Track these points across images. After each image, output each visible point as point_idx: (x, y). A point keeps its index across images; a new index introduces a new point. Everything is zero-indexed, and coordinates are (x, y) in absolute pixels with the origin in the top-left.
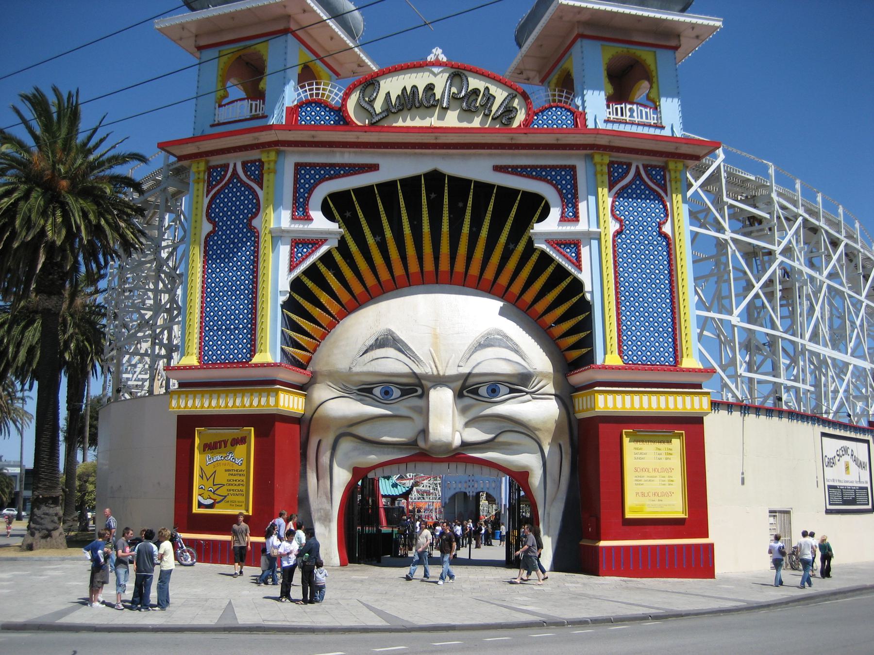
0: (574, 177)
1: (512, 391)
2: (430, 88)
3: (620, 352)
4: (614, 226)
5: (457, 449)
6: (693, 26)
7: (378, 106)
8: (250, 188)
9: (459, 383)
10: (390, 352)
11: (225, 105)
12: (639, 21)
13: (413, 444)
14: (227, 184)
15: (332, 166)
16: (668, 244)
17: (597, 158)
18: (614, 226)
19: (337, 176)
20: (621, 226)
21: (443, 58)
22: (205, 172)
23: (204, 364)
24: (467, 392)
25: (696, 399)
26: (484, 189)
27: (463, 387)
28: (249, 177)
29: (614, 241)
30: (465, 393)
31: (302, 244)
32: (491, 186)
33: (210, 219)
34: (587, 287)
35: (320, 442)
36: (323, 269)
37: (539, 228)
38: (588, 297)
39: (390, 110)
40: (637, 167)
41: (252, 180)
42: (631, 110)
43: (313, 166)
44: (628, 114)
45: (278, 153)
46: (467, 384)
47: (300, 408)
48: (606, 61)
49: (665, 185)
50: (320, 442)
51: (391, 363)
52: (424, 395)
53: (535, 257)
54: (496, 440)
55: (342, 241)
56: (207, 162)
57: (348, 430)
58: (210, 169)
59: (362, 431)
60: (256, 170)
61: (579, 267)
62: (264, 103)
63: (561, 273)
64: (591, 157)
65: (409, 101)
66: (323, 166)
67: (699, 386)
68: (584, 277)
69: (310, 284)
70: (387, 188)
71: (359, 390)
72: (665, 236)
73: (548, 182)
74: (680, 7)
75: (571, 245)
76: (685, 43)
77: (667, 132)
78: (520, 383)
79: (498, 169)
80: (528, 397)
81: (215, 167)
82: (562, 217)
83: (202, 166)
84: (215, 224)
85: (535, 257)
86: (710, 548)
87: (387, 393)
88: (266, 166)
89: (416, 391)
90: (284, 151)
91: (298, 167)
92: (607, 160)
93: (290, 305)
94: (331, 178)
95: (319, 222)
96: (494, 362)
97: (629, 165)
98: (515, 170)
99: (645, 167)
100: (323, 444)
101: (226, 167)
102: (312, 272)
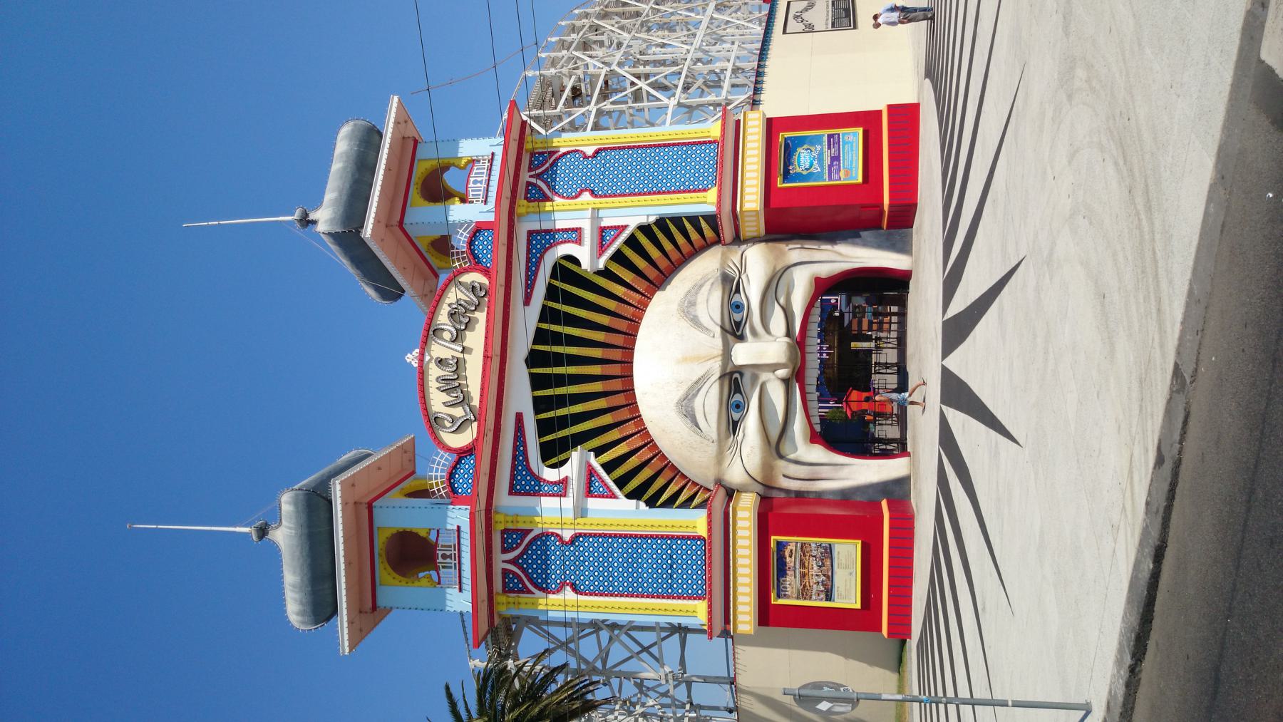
1: (738, 291)
3: (705, 190)
4: (586, 196)
6: (397, 123)
7: (458, 412)
8: (530, 542)
9: (730, 338)
10: (698, 403)
13: (786, 381)
14: (524, 571)
16: (605, 149)
18: (586, 196)
19: (525, 453)
23: (706, 595)
25: (749, 123)
26: (547, 315)
27: (734, 334)
31: (590, 487)
34: (643, 220)
37: (586, 264)
38: (652, 219)
42: (475, 182)
43: (513, 477)
45: (497, 512)
51: (709, 401)
52: (740, 370)
57: (775, 445)
58: (507, 590)
59: (774, 433)
60: (513, 536)
61: (624, 227)
64: (520, 216)
65: (453, 385)
66: (514, 467)
67: (738, 122)
70: (540, 405)
72: (597, 152)
73: (542, 256)
74: (377, 137)
76: (411, 133)
77: (499, 151)
78: (731, 284)
79: (527, 301)
80: (743, 277)
86: (890, 107)
87: (738, 406)
88: (510, 526)
93: (651, 503)
94: (526, 459)
96: (711, 306)
99: (530, 169)
100: (787, 473)
101: (505, 572)
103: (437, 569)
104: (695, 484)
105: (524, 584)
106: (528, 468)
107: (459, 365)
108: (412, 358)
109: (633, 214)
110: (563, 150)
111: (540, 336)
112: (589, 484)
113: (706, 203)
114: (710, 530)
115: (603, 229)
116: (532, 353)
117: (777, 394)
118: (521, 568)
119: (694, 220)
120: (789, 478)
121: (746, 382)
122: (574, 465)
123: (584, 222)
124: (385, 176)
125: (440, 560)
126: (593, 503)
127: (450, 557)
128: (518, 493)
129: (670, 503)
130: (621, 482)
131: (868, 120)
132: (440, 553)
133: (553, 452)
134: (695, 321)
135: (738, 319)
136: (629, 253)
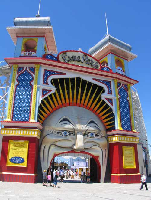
0: (110, 84)
1: (96, 135)
2: (79, 57)
7: (67, 59)
8: (31, 74)
12: (123, 52)
13: (72, 148)
15: (54, 72)
21: (82, 51)
22: (17, 68)
24: (86, 134)
26: (90, 84)
28: (30, 71)
31: (45, 92)
32: (92, 83)
33: (17, 81)
35: (45, 146)
36: (49, 98)
39: (70, 60)
41: (31, 72)
45: (40, 66)
50: (45, 146)
53: (101, 102)
54: (92, 148)
56: (18, 65)
58: (19, 68)
59: (58, 144)
60: (33, 70)
63: (107, 106)
68: (113, 108)
69: (45, 102)
70: (67, 80)
71: (58, 132)
72: (128, 101)
76: (129, 60)
79: (94, 79)
81: (20, 67)
83: (16, 66)
84: (19, 82)
85: (101, 102)
87: (65, 133)
88: (36, 69)
90: (41, 66)
91: (45, 70)
93: (40, 107)
100: (46, 148)
101: (23, 68)
102: (46, 99)
103: (25, 52)
105: (20, 72)
106: (51, 75)
107: (79, 61)
108: (80, 49)
109: (115, 108)
110: (128, 92)
112: (46, 90)
117: (68, 144)
118: (24, 71)
119: (114, 124)
125: (28, 52)
127: (29, 55)
128: (45, 72)
129: (39, 112)
132: (30, 52)
135: (89, 135)
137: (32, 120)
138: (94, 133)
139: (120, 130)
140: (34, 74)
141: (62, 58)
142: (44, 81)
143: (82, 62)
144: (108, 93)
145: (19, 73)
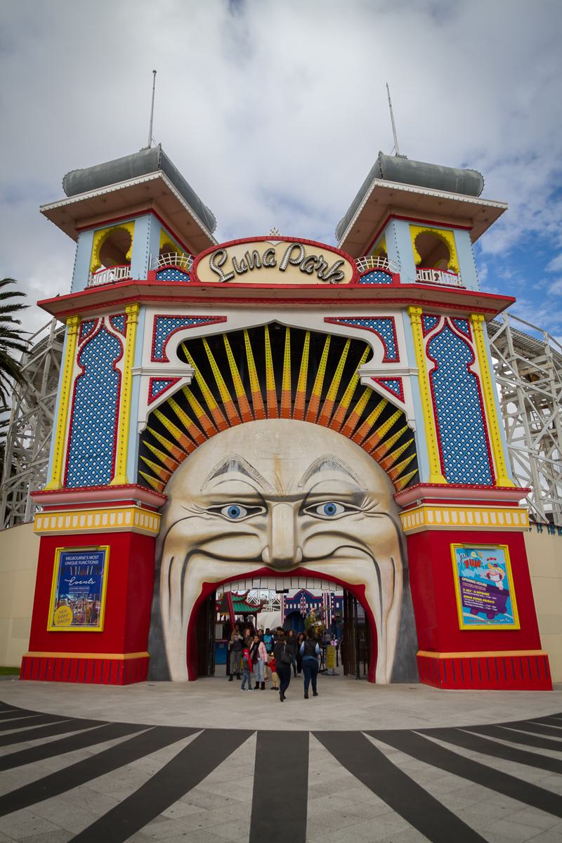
0: (393, 326)
1: (347, 509)
3: (443, 473)
5: (297, 564)
8: (115, 336)
11: (97, 273)
14: (96, 334)
16: (478, 382)
17: (412, 310)
20: (436, 366)
23: (66, 488)
24: (306, 510)
25: (515, 515)
26: (318, 338)
27: (303, 506)
29: (431, 378)
30: (304, 511)
34: (409, 417)
35: (173, 558)
37: (363, 366)
38: (411, 424)
40: (446, 319)
41: (116, 330)
42: (436, 275)
44: (434, 278)
46: (306, 503)
47: (155, 528)
48: (414, 236)
49: (470, 333)
50: (173, 558)
51: (236, 484)
54: (334, 555)
55: (194, 380)
56: (80, 317)
57: (197, 548)
61: (402, 399)
62: (130, 269)
70: (236, 337)
71: (209, 510)
72: (475, 375)
75: (395, 383)
78: (354, 502)
79: (328, 320)
80: (361, 515)
82: (385, 358)
84: (84, 368)
86: (545, 658)
89: (261, 510)
92: (420, 311)
93: (145, 435)
95: (175, 363)
96: (330, 483)
97: (438, 317)
98: (342, 322)
100: (175, 561)
104: (169, 477)
109: (416, 406)
110: (473, 346)
111: (298, 334)
113: (430, 471)
114: (119, 487)
115: (399, 380)
116: (283, 328)
119: (414, 464)
120: (171, 561)
121: (258, 519)
122: (185, 372)
123: (405, 359)
124: (433, 197)
126: (145, 383)
128: (156, 322)
129: (143, 451)
130: (165, 408)
131: (529, 634)
133: (193, 349)
134: (316, 469)
136: (380, 409)
137: (119, 480)
138: (336, 501)
139: (437, 486)
140: (125, 336)
141: (212, 270)
142: (153, 353)
143: (283, 267)
144: (386, 360)
145: (84, 342)
